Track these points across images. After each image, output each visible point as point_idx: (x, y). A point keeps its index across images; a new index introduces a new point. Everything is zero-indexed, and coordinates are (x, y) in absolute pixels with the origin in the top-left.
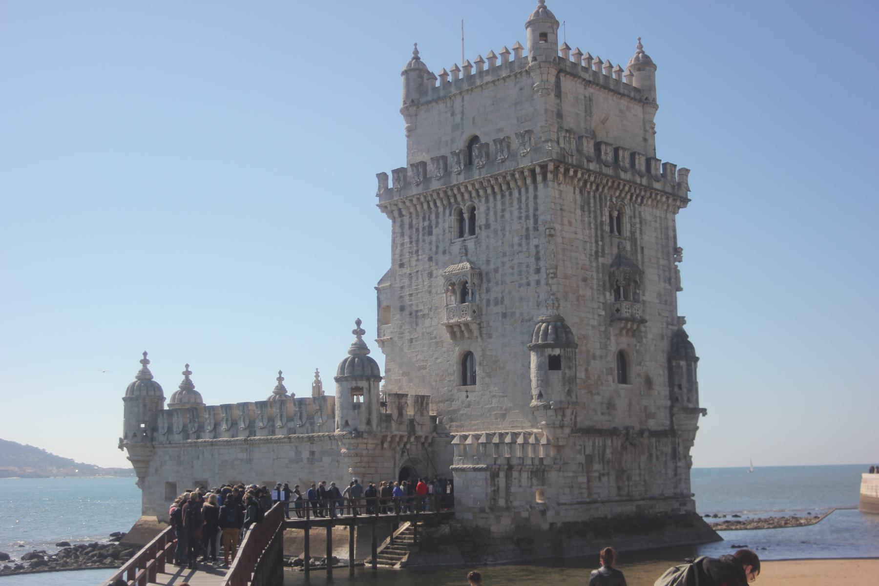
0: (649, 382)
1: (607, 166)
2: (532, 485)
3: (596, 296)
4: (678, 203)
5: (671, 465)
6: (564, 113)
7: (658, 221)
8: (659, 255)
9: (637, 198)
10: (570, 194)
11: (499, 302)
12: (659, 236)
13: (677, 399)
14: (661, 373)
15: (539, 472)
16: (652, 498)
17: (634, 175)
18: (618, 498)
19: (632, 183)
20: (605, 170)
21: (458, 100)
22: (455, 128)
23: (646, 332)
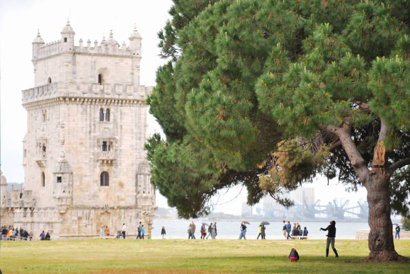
1: (95, 94)
3: (88, 150)
9: (118, 103)
10: (75, 108)
11: (50, 153)
12: (134, 119)
13: (139, 192)
20: (94, 96)
21: (46, 61)
22: (46, 73)
23: (121, 164)
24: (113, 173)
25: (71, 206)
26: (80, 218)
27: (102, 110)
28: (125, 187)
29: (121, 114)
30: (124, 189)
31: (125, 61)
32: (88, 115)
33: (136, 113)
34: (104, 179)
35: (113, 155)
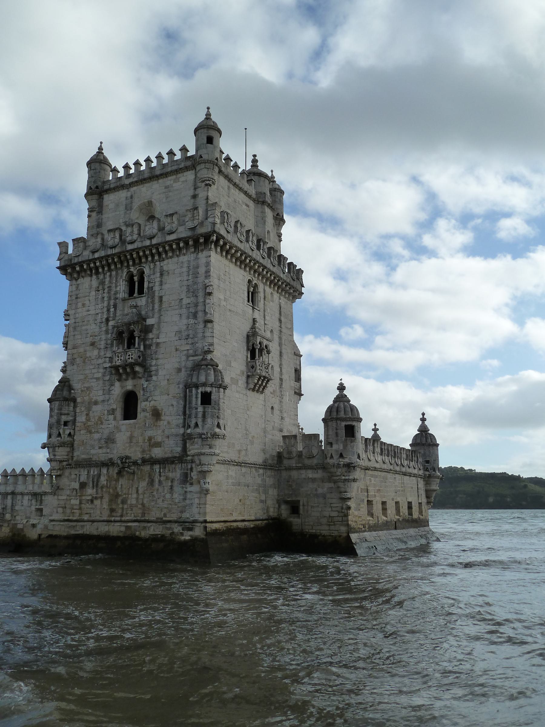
0: (157, 414)
1: (111, 248)
2: (31, 505)
3: (102, 353)
4: (202, 240)
5: (178, 489)
6: (104, 220)
7: (186, 265)
8: (183, 296)
9: (153, 255)
12: (185, 278)
14: (175, 403)
15: (37, 496)
16: (148, 521)
17: (142, 241)
18: (105, 518)
19: (137, 250)
23: (157, 371)
24: (142, 392)
25: (70, 462)
26: (83, 485)
27: (131, 277)
28: (163, 418)
29: (162, 275)
30: (162, 422)
31: (182, 179)
32: (106, 291)
33: (188, 267)
34: (130, 406)
35: (135, 356)
